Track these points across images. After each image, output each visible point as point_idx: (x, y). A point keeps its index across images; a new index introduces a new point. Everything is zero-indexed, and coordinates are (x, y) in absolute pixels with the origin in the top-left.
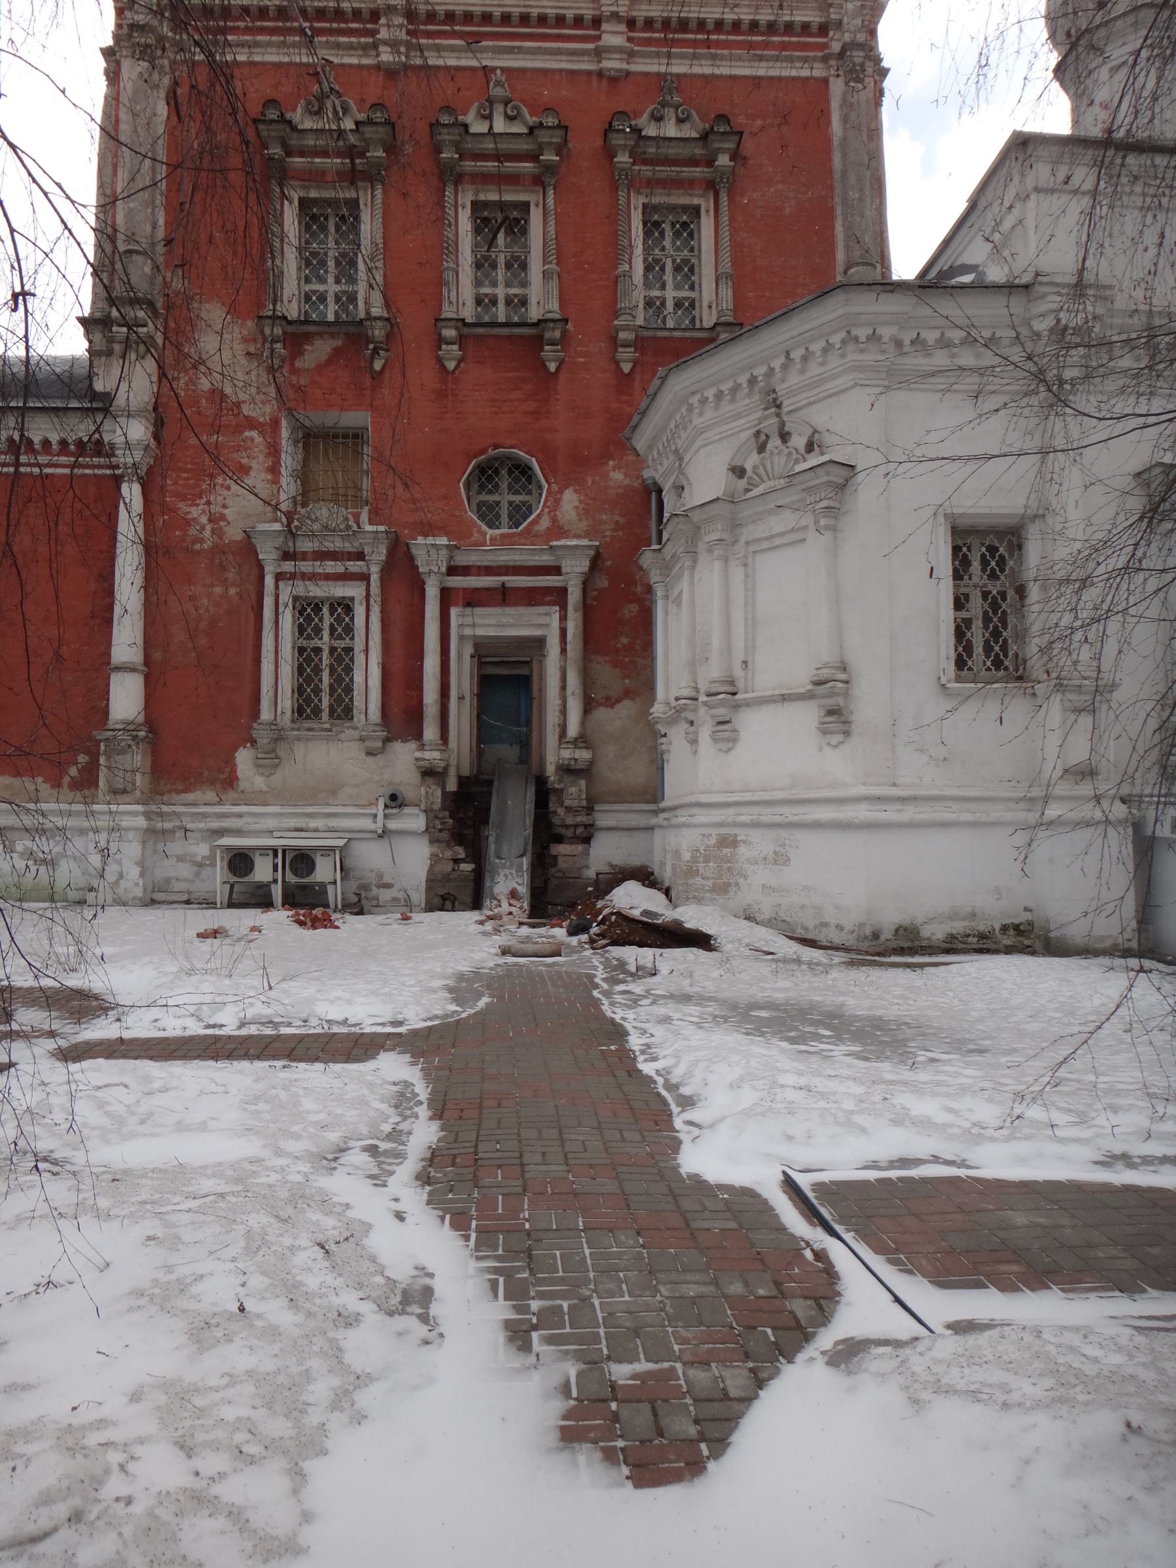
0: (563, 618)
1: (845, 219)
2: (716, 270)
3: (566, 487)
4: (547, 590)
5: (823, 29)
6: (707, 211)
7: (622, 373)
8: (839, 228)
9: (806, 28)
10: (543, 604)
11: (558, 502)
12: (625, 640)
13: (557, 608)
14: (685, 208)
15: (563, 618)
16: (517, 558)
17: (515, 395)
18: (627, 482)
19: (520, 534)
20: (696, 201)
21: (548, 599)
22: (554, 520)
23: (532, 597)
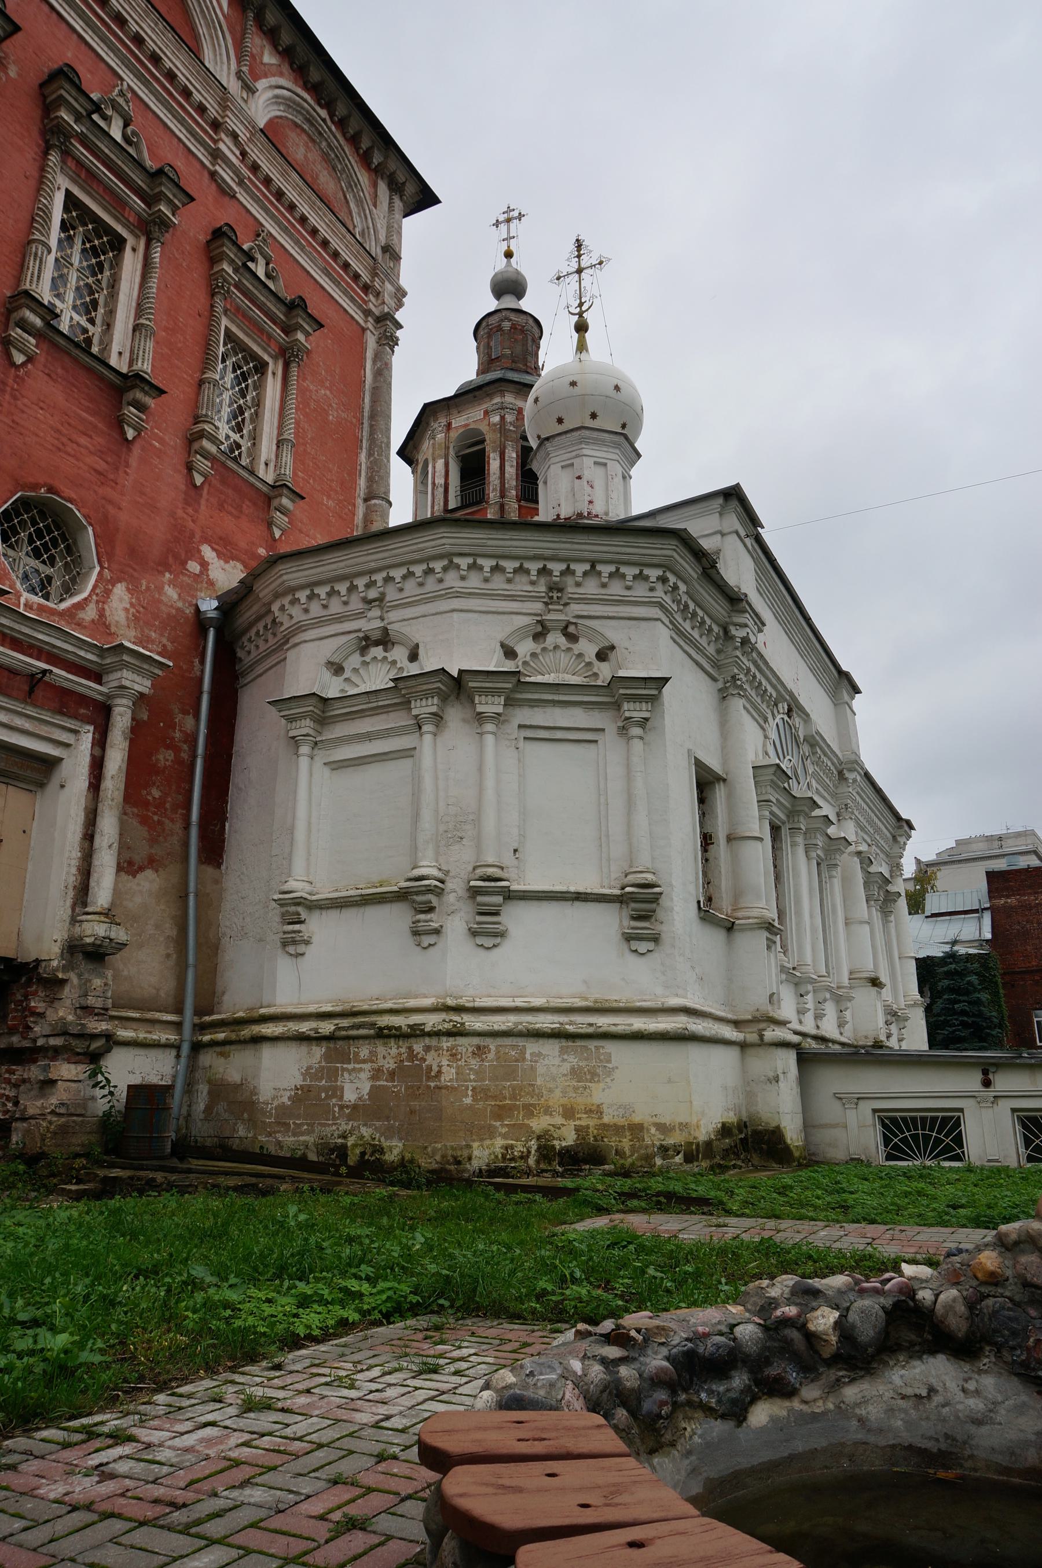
0: (101, 742)
1: (370, 454)
2: (280, 434)
3: (119, 580)
4: (83, 700)
5: (366, 288)
6: (274, 374)
7: (195, 486)
8: (363, 457)
9: (356, 277)
10: (75, 717)
11: (108, 593)
12: (156, 793)
13: (92, 728)
14: (254, 357)
15: (101, 742)
16: (58, 643)
17: (83, 440)
18: (180, 604)
19: (62, 614)
20: (266, 357)
21: (82, 711)
22: (102, 614)
23: (66, 703)
